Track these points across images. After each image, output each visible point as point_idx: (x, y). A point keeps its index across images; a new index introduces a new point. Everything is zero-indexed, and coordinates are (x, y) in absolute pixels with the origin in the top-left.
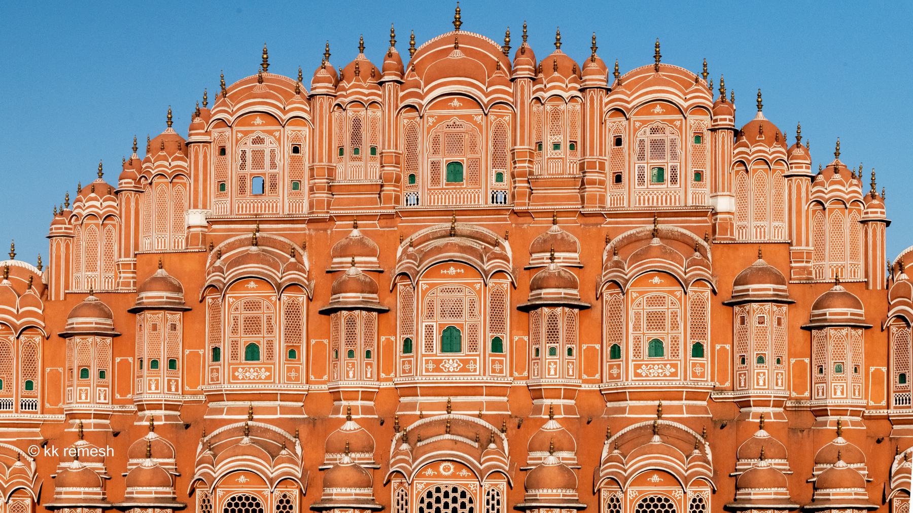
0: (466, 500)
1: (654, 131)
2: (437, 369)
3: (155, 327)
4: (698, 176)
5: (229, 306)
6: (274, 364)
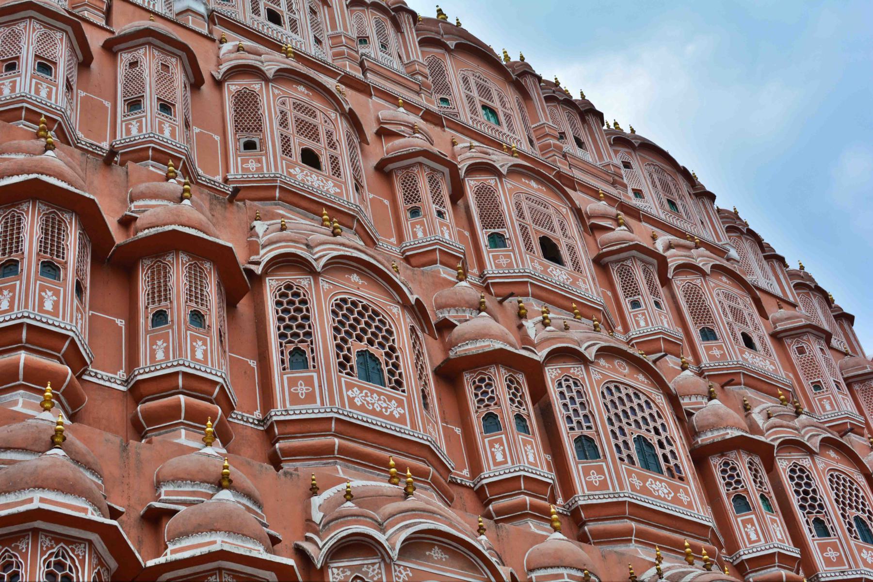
3: (165, 67)
6: (345, 183)
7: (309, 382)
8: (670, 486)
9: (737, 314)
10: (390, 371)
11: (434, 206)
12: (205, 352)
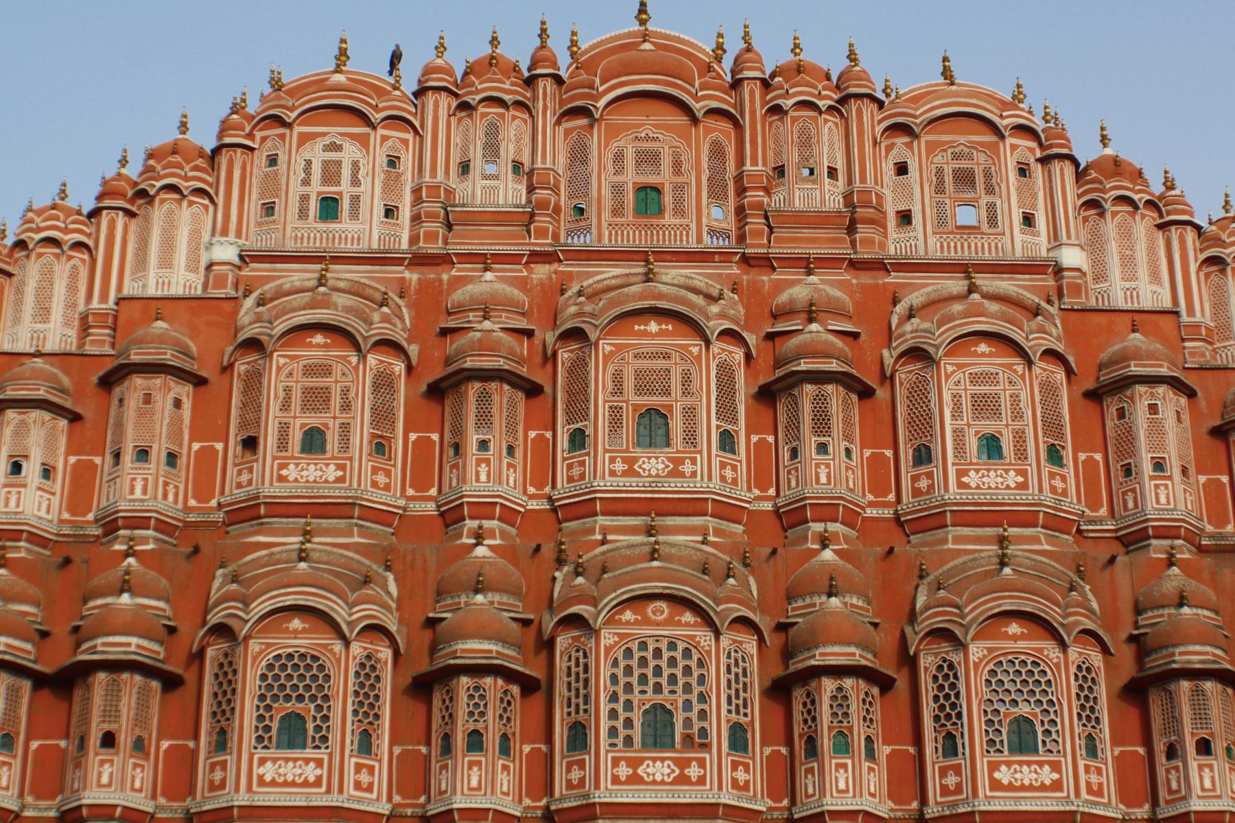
0: (693, 664)
1: (956, 157)
2: (630, 472)
3: (148, 399)
4: (1028, 220)
5: (279, 369)
6: (351, 459)
7: (224, 765)
8: (677, 761)
9: (985, 406)
10: (318, 728)
11: (475, 437)
12: (111, 774)
